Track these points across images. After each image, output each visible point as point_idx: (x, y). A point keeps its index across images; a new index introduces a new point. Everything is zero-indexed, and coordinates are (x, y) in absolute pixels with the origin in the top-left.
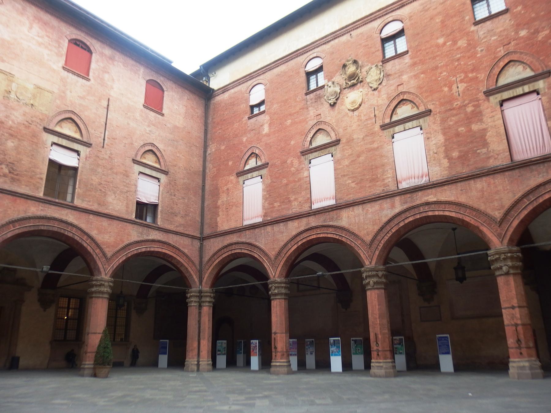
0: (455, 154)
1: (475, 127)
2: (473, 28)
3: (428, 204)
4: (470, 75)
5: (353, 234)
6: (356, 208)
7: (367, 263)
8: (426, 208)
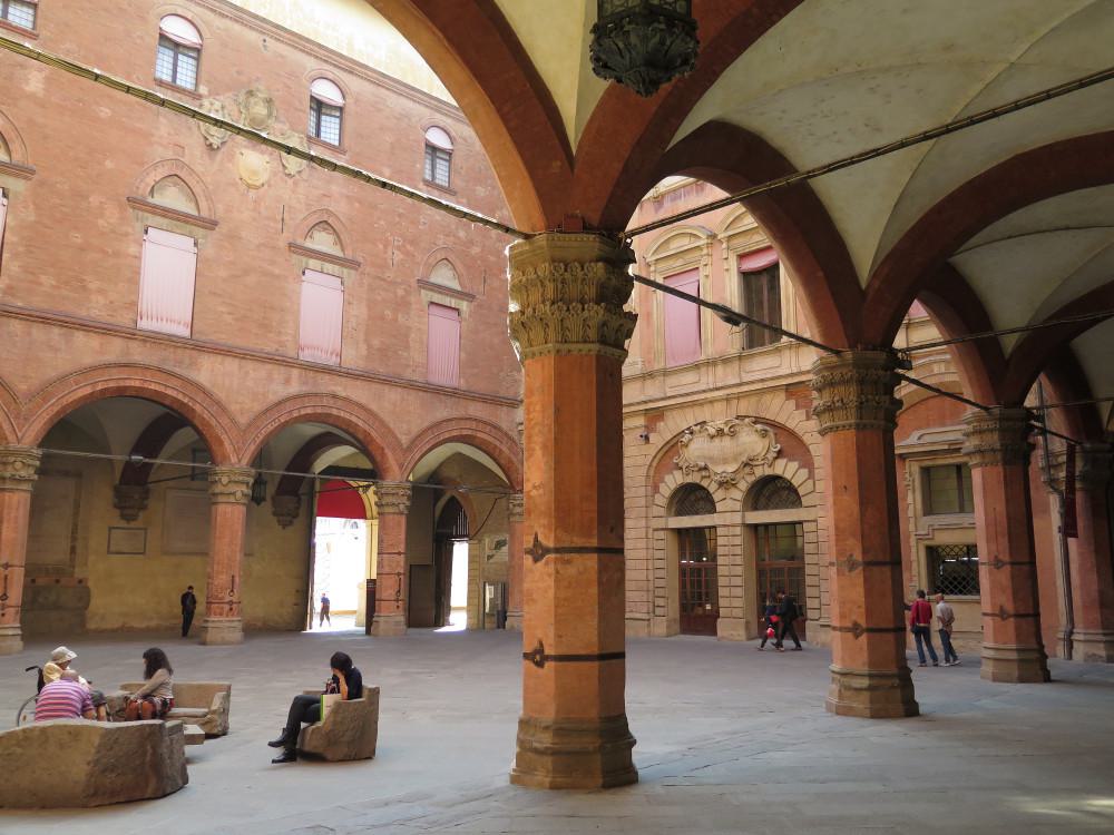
0: (376, 342)
3: (335, 396)
4: (408, 247)
5: (218, 403)
6: (229, 360)
7: (234, 459)
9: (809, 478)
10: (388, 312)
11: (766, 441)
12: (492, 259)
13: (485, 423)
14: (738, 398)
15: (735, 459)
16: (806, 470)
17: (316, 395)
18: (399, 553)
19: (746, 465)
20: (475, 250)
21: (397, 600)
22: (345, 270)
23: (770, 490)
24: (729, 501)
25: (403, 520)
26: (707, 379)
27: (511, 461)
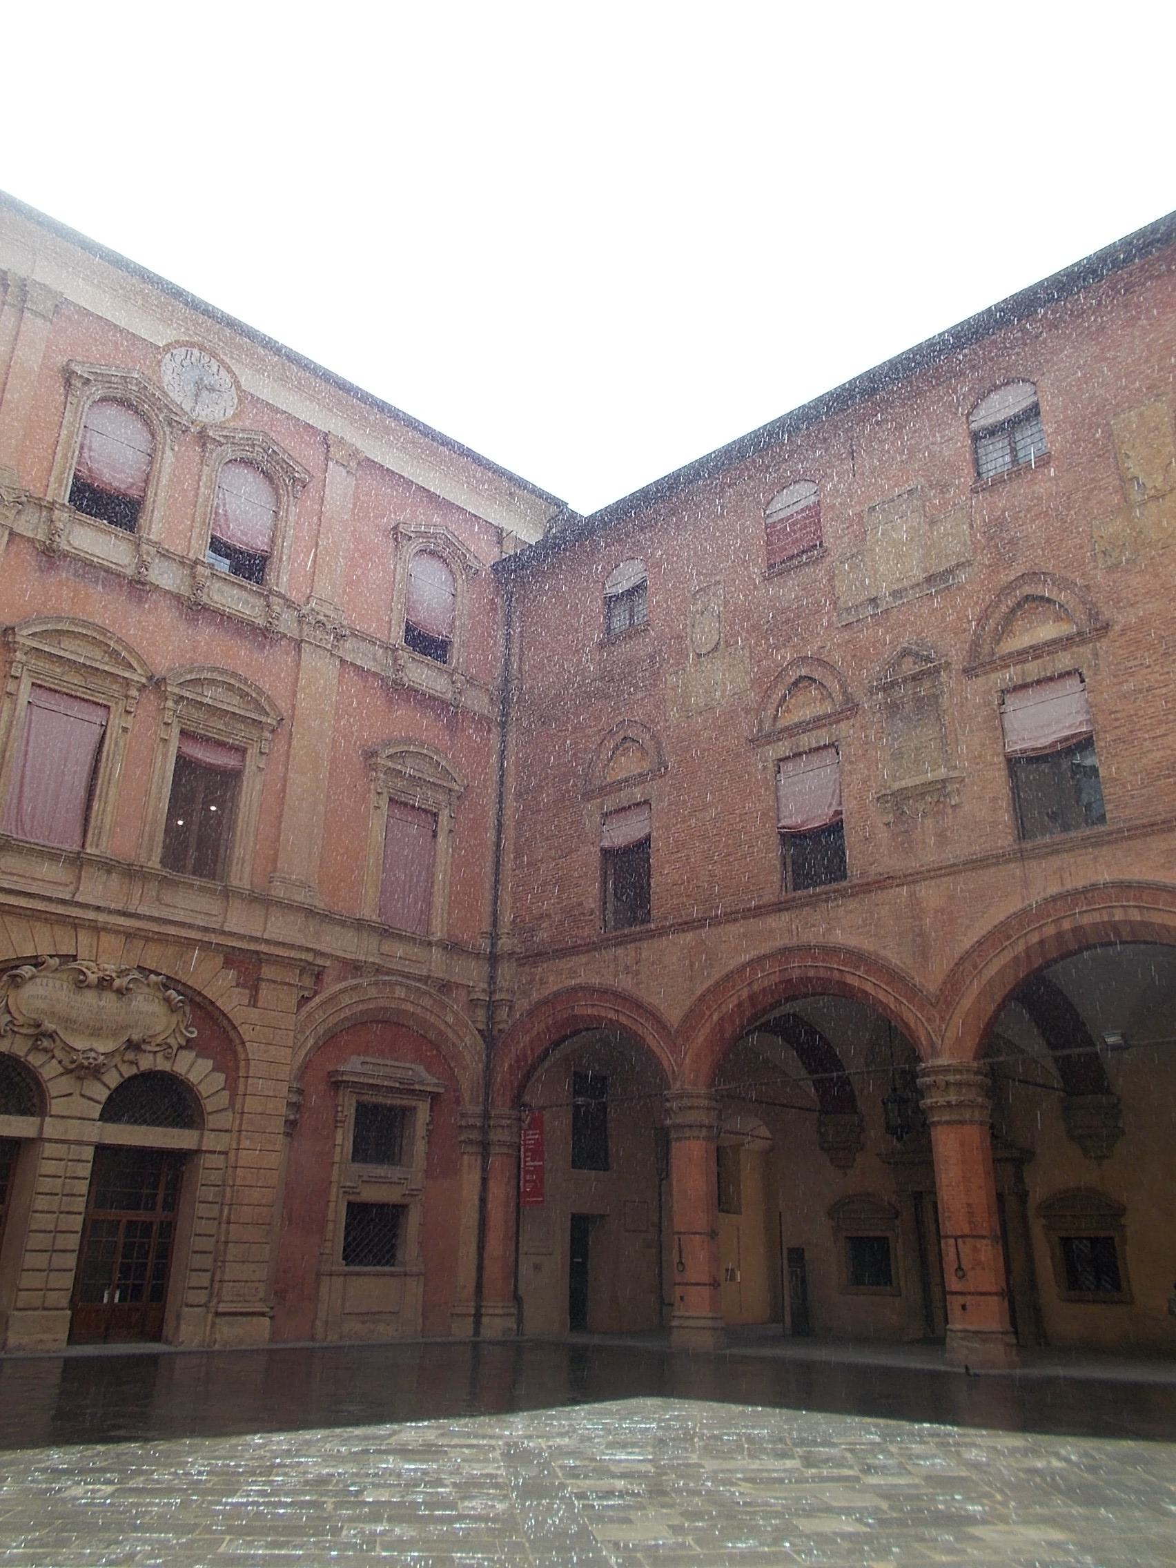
9: (224, 1089)
11: (174, 1019)
14: (147, 939)
15: (115, 1034)
16: (223, 1077)
19: (132, 1046)
23: (153, 1094)
24: (76, 1097)
26: (96, 890)
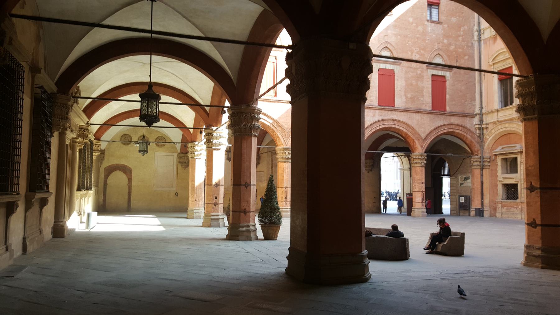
0: (409, 96)
1: (420, 84)
2: (426, 23)
3: (393, 120)
4: (422, 52)
8: (392, 122)
10: (414, 82)
12: (460, 50)
13: (459, 126)
17: (385, 120)
18: (423, 183)
20: (452, 48)
21: (422, 202)
22: (395, 66)
25: (424, 169)
27: (471, 142)
